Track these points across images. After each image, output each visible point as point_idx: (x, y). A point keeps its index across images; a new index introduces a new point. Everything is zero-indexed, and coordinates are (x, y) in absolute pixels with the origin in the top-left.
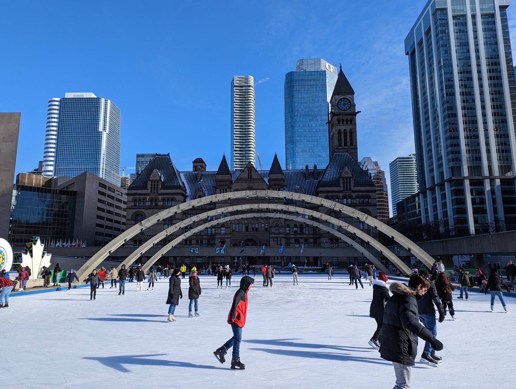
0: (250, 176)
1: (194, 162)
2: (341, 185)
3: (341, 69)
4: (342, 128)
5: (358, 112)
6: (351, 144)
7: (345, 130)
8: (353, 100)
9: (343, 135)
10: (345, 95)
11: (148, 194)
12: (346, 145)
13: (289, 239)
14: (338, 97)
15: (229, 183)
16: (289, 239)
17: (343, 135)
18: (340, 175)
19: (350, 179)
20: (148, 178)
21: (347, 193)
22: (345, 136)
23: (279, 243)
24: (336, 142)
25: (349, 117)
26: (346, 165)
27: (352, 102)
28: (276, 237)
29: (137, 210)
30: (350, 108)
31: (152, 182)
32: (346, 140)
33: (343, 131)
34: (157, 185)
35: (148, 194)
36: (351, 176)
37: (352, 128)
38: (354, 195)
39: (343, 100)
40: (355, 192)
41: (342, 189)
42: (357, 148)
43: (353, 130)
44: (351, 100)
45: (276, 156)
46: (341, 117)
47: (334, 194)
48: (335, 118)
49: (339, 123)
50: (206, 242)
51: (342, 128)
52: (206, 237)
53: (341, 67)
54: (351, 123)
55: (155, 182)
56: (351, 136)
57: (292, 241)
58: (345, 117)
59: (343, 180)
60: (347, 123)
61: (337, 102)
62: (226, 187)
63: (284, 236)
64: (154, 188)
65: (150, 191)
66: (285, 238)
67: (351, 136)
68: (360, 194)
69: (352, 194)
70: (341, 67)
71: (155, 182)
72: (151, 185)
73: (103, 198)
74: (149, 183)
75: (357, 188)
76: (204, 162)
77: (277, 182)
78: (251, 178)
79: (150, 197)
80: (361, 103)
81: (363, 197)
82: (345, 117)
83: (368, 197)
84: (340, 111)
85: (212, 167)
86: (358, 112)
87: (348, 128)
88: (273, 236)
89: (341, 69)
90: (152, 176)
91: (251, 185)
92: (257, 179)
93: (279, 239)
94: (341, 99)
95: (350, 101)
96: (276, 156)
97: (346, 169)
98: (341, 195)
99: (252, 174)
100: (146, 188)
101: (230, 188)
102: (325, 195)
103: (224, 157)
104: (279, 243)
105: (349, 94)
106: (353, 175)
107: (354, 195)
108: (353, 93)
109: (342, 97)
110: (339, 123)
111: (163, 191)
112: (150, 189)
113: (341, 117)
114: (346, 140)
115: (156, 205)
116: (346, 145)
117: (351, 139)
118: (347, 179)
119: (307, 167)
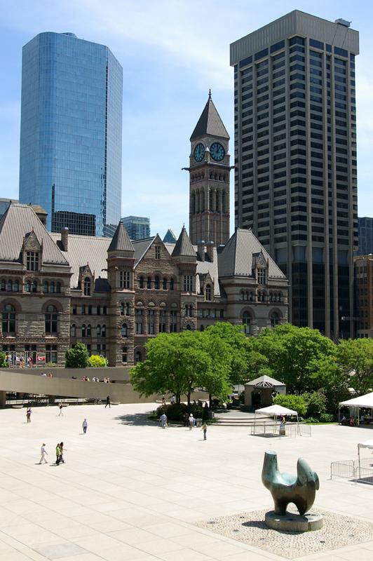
3: (210, 97)
22: (217, 197)
25: (223, 171)
29: (6, 297)
31: (28, 254)
38: (268, 291)
41: (257, 283)
47: (249, 288)
52: (96, 340)
53: (210, 95)
55: (33, 254)
67: (223, 197)
70: (210, 95)
71: (33, 254)
72: (28, 259)
74: (25, 255)
83: (280, 295)
89: (210, 97)
94: (214, 144)
95: (223, 149)
102: (240, 288)
115: (35, 290)
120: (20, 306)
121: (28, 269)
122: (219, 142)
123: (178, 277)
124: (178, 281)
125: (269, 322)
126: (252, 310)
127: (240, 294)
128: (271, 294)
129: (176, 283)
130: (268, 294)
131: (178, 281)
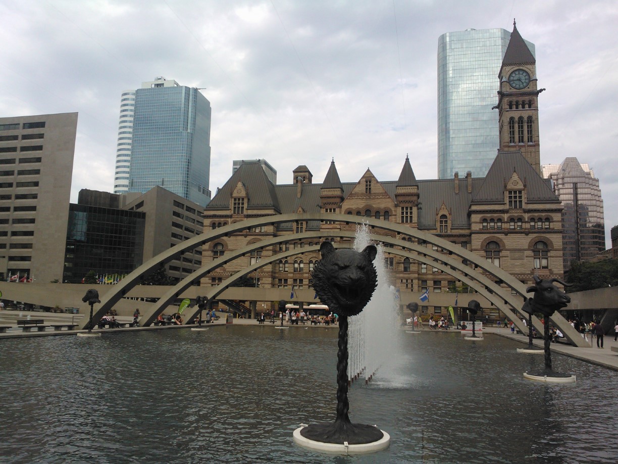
0: (368, 189)
1: (294, 172)
2: (507, 200)
3: (515, 27)
4: (516, 114)
5: (541, 91)
6: (530, 139)
7: (521, 118)
8: (534, 72)
9: (516, 126)
10: (520, 64)
11: (231, 216)
12: (521, 140)
13: (424, 281)
14: (509, 69)
15: (338, 200)
16: (424, 281)
17: (516, 126)
18: (505, 187)
19: (520, 192)
20: (231, 194)
21: (516, 214)
23: (409, 286)
24: (507, 137)
25: (527, 98)
26: (515, 171)
27: (531, 75)
28: (404, 278)
30: (528, 84)
31: (235, 200)
32: (521, 132)
33: (516, 119)
34: (243, 204)
35: (231, 216)
37: (531, 114)
39: (517, 73)
40: (529, 211)
41: (507, 207)
42: (538, 145)
43: (534, 118)
44: (529, 72)
45: (407, 159)
46: (514, 99)
48: (506, 100)
49: (511, 108)
50: (307, 283)
51: (516, 114)
53: (515, 24)
54: (530, 107)
56: (530, 127)
57: (430, 283)
58: (521, 99)
59: (510, 192)
60: (523, 107)
61: (508, 76)
62: (334, 206)
63: (416, 275)
64: (239, 208)
65: (232, 212)
66: (419, 279)
67: (530, 127)
68: (536, 214)
69: (523, 214)
70: (515, 24)
71: (239, 199)
72: (235, 204)
73: (179, 220)
75: (531, 207)
76: (309, 172)
77: (408, 198)
78: (370, 192)
79: (232, 219)
80: (545, 75)
81: (540, 220)
82: (521, 99)
84: (513, 90)
85: (319, 178)
86: (541, 91)
87: (525, 114)
88: (401, 275)
89: (515, 27)
90: (235, 191)
91: (371, 202)
92: (379, 194)
93: (409, 281)
95: (528, 74)
96: (407, 159)
97: (515, 177)
98: (506, 217)
99: (372, 187)
100: (227, 208)
101: (340, 207)
103: (333, 163)
104: (409, 286)
105: (527, 63)
106: (525, 186)
107: (526, 216)
108: (532, 62)
109: (516, 68)
110: (511, 108)
111: (250, 212)
112: (233, 209)
113: (514, 99)
114: (521, 132)
116: (521, 140)
117: (530, 132)
118: (515, 192)
119: (456, 175)
120: (227, 244)
121: (234, 213)
122: (521, 68)
123: (393, 209)
124: (394, 213)
126: (501, 240)
127: (480, 223)
129: (391, 216)
131: (394, 213)
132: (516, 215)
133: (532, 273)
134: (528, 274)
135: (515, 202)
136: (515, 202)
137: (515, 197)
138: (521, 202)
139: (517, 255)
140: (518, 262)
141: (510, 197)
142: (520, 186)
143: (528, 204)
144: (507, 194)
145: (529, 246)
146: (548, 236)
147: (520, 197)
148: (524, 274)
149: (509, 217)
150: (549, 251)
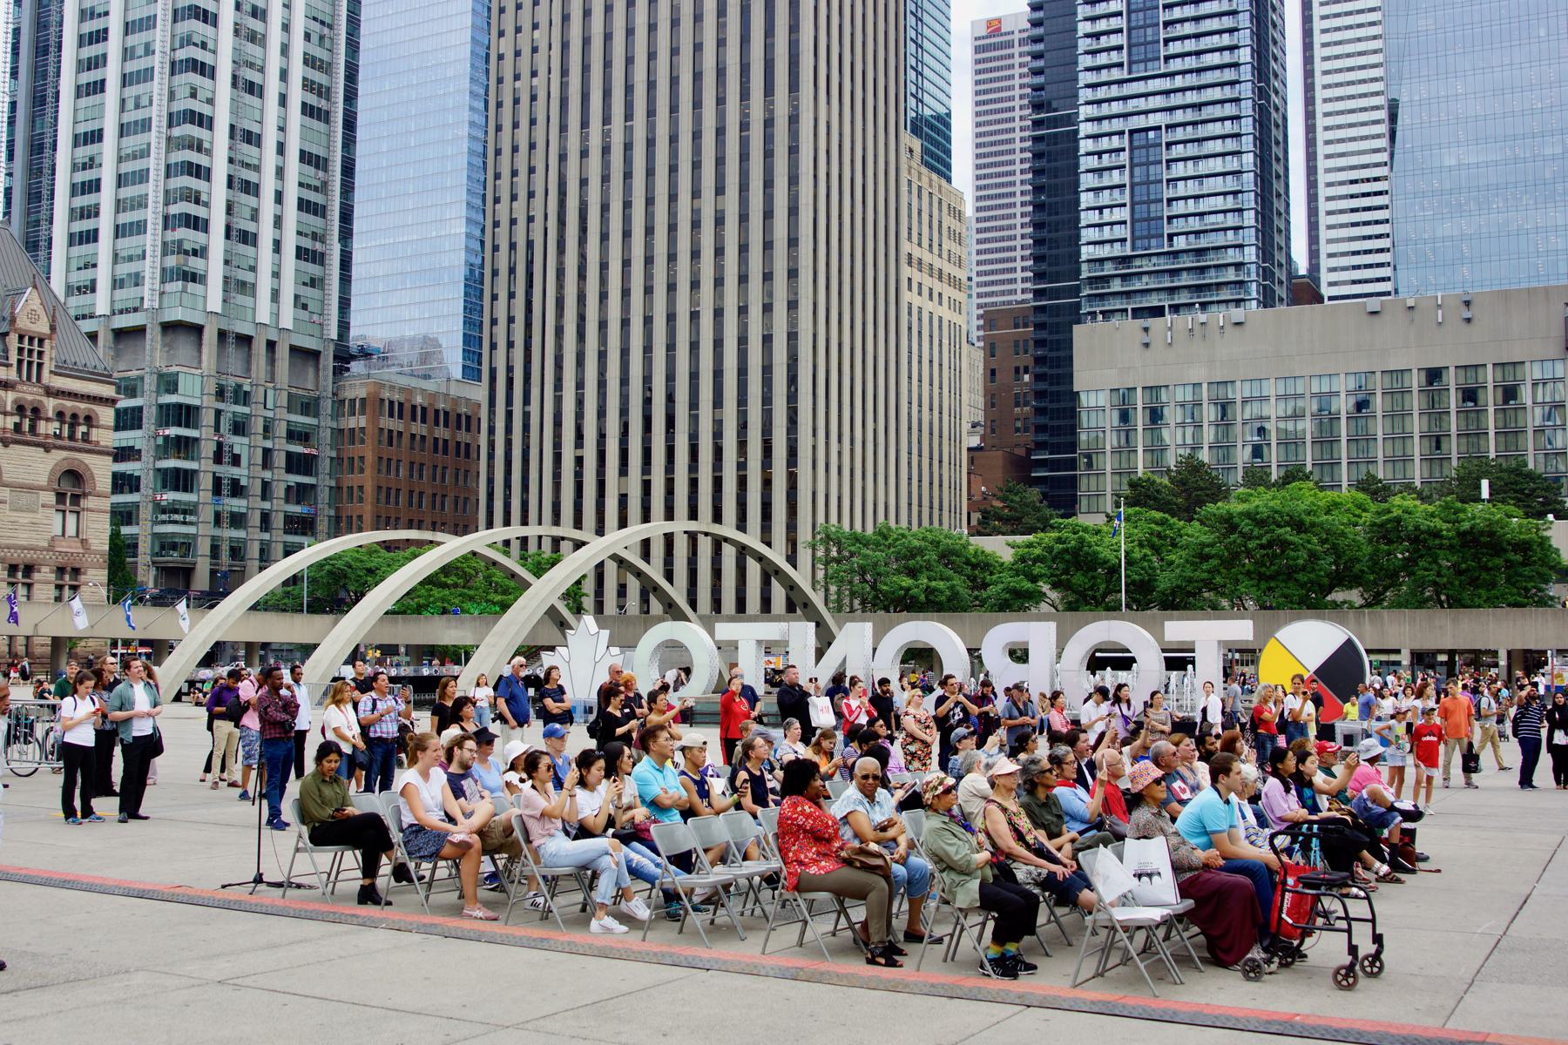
2: (14, 358)
18: (13, 320)
19: (41, 341)
21: (30, 394)
36: (46, 330)
38: (51, 405)
41: (12, 375)
59: (21, 338)
69: (44, 399)
83: (89, 420)
106: (53, 328)
107: (51, 405)
118: (31, 339)
125: (50, 498)
128: (60, 415)
130: (50, 414)
132: (30, 397)
133: (51, 548)
134: (44, 549)
135: (30, 364)
136: (30, 364)
137: (31, 352)
138: (40, 365)
139: (25, 498)
140: (25, 518)
141: (21, 350)
142: (43, 327)
143: (56, 374)
144: (13, 340)
145: (50, 481)
146: (88, 459)
147: (40, 354)
148: (34, 549)
149: (15, 401)
150: (85, 495)
